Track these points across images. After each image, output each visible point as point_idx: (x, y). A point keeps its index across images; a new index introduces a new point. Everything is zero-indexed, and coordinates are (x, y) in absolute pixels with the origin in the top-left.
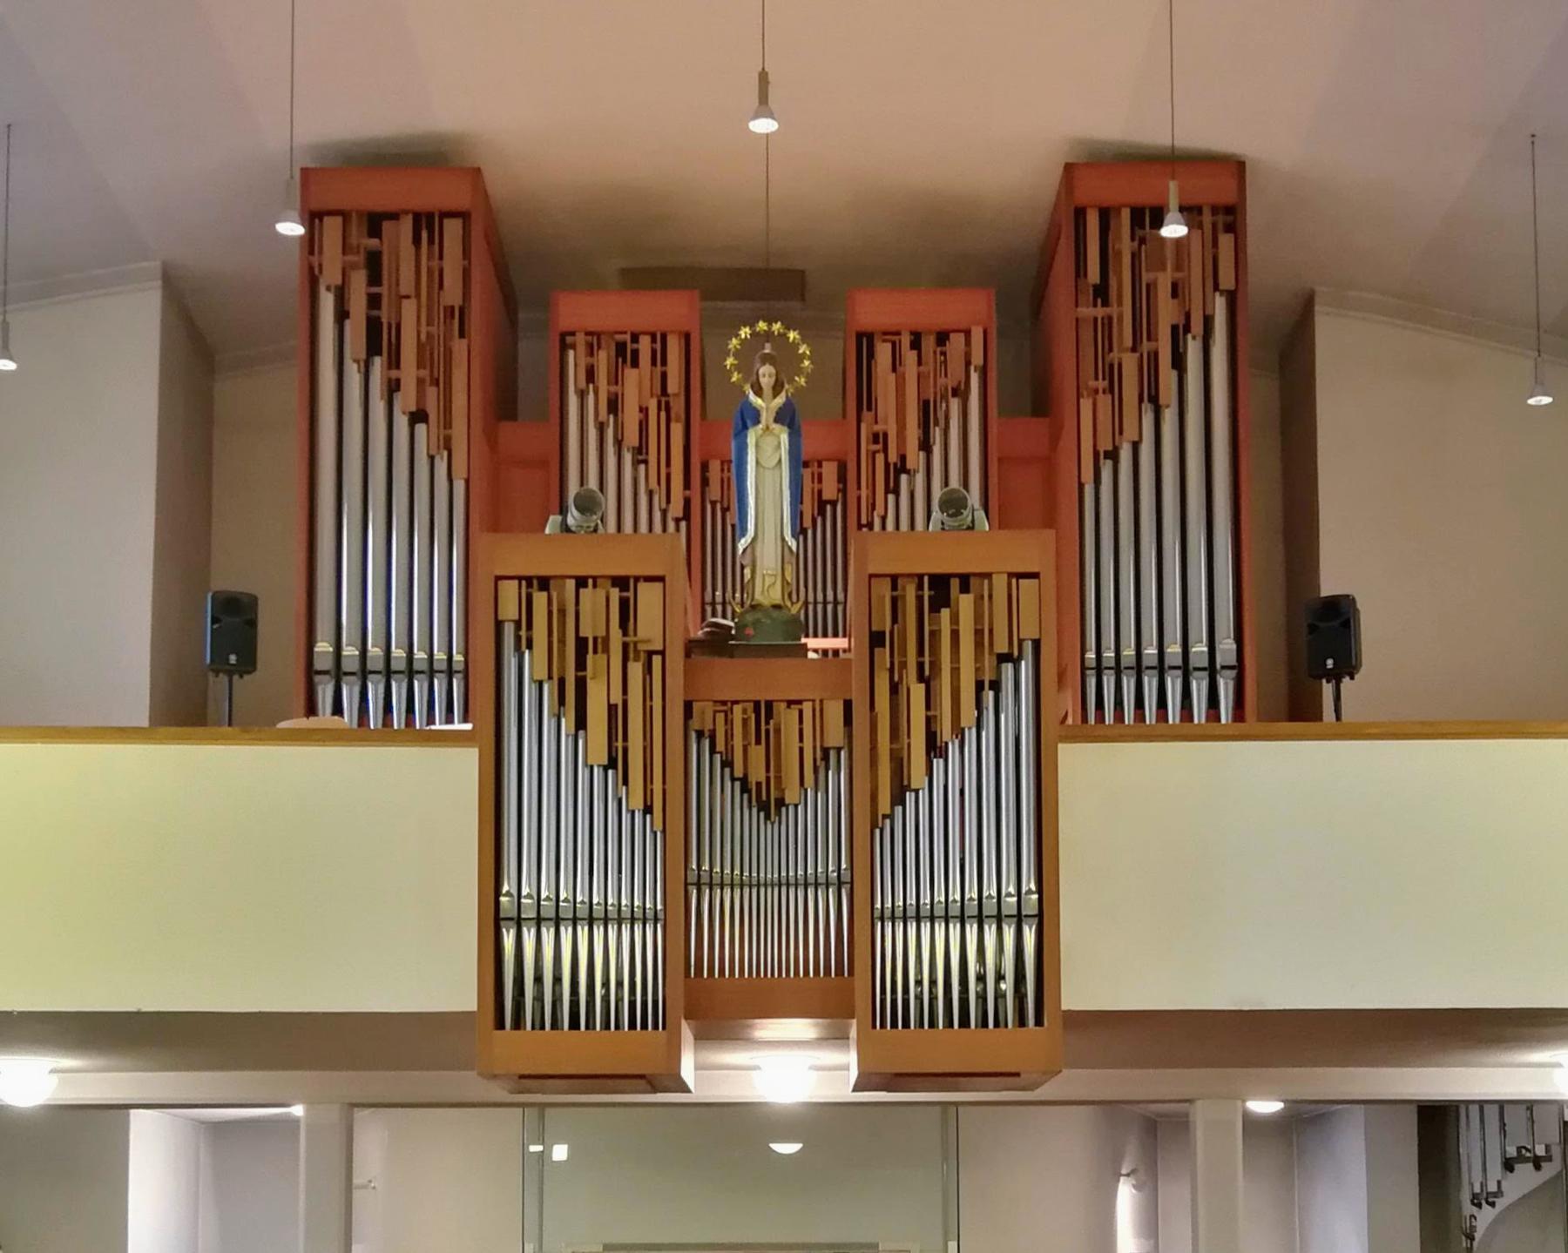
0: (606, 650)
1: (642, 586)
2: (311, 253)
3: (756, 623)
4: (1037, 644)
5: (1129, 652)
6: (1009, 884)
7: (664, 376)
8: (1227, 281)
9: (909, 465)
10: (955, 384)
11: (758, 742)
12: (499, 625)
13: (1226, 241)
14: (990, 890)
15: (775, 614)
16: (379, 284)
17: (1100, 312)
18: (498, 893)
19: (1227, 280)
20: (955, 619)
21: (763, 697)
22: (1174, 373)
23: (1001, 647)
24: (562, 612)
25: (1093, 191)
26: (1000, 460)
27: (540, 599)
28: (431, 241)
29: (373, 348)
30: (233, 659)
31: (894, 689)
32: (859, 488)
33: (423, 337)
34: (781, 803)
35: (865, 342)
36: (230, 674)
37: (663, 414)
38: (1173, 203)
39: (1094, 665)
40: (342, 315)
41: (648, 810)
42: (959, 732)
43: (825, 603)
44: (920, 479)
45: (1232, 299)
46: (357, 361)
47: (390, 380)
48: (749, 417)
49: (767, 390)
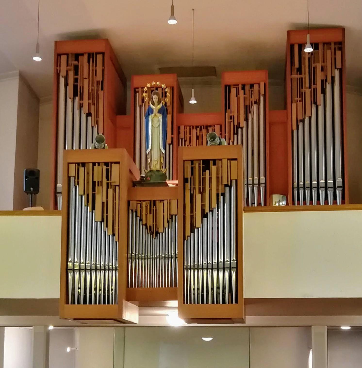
0: (102, 185)
1: (113, 165)
2: (57, 66)
3: (151, 176)
4: (236, 181)
6: (225, 257)
8: (339, 65)
9: (241, 126)
11: (150, 213)
12: (69, 178)
13: (339, 53)
14: (221, 260)
15: (156, 173)
16: (77, 75)
17: (299, 76)
18: (67, 261)
19: (339, 65)
20: (210, 174)
21: (152, 199)
22: (322, 95)
23: (225, 182)
24: (88, 173)
25: (296, 39)
26: (269, 123)
27: (82, 169)
28: (93, 61)
29: (75, 94)
30: (32, 189)
31: (192, 196)
32: (225, 133)
33: (90, 91)
34: (157, 233)
35: (228, 88)
36: (31, 194)
38: (308, 41)
40: (66, 85)
41: (114, 235)
42: (211, 210)
44: (244, 130)
45: (341, 71)
46: (70, 98)
47: (80, 104)
48: (150, 112)
49: (156, 104)
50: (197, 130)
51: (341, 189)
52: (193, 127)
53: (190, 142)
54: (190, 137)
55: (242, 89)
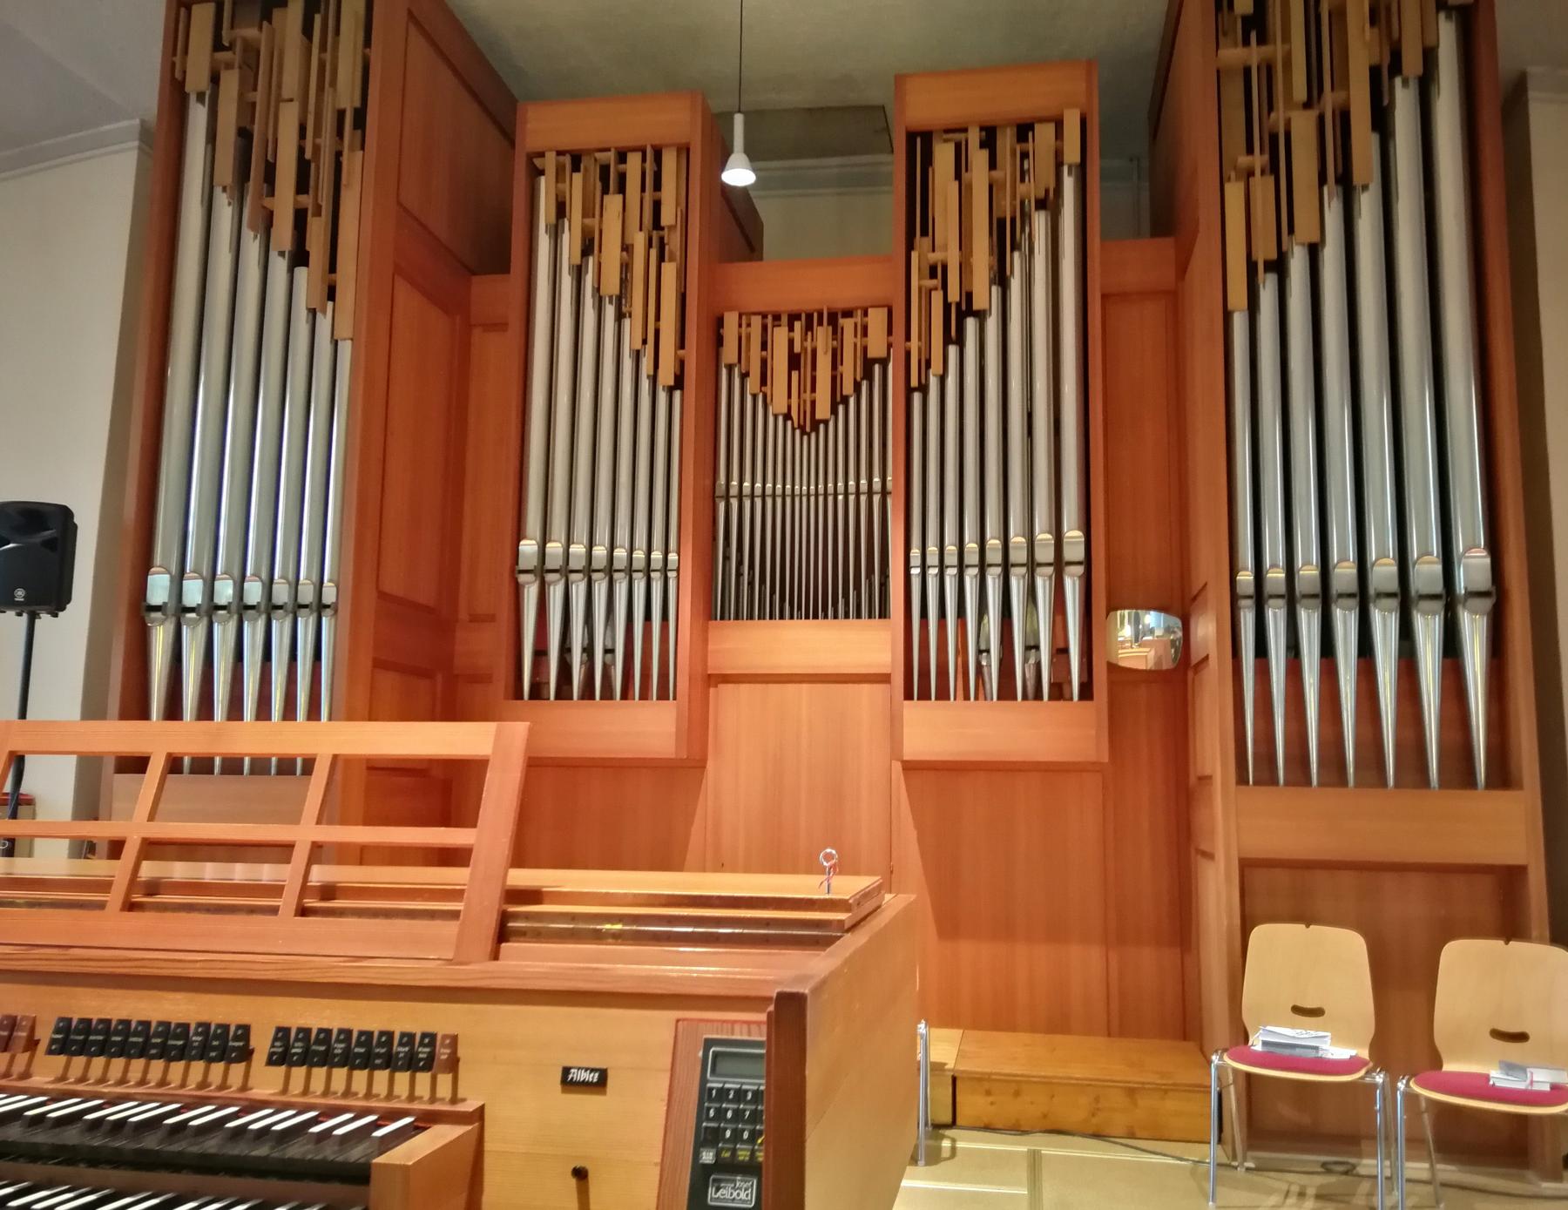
5: (1308, 572)
7: (657, 205)
9: (976, 306)
10: (1042, 194)
17: (1254, 55)
22: (1374, 139)
32: (908, 338)
37: (654, 253)
39: (1251, 590)
43: (870, 493)
44: (992, 324)
50: (791, 329)
51: (1487, 604)
52: (777, 317)
53: (763, 382)
54: (764, 362)
55: (982, 146)
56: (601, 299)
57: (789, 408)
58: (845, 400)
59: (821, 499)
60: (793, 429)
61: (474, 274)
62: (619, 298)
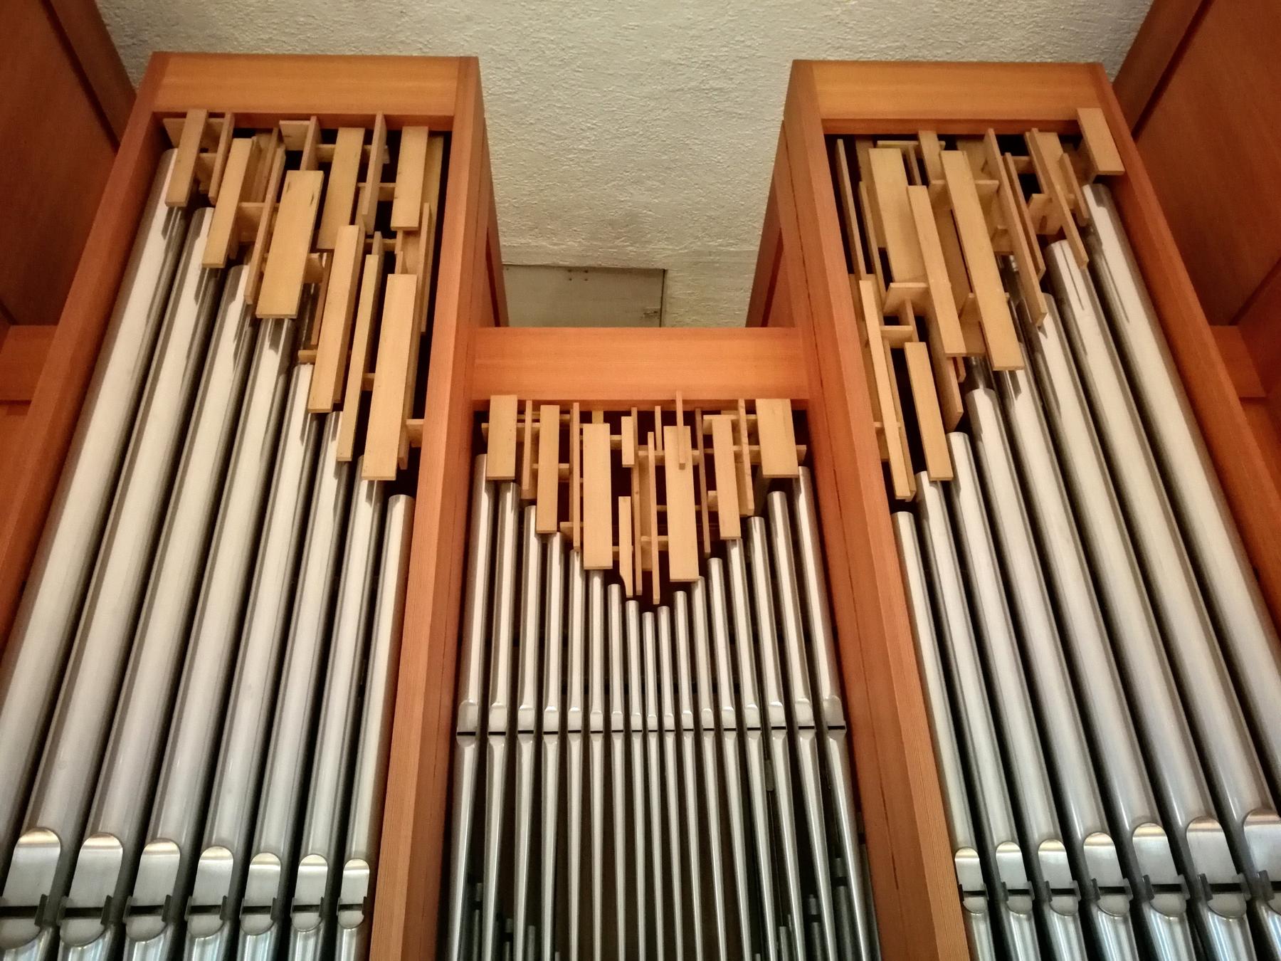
37: (373, 262)
53: (564, 513)
56: (256, 324)
57: (616, 557)
58: (720, 549)
59: (688, 741)
60: (624, 599)
61: (14, 322)
62: (297, 323)
